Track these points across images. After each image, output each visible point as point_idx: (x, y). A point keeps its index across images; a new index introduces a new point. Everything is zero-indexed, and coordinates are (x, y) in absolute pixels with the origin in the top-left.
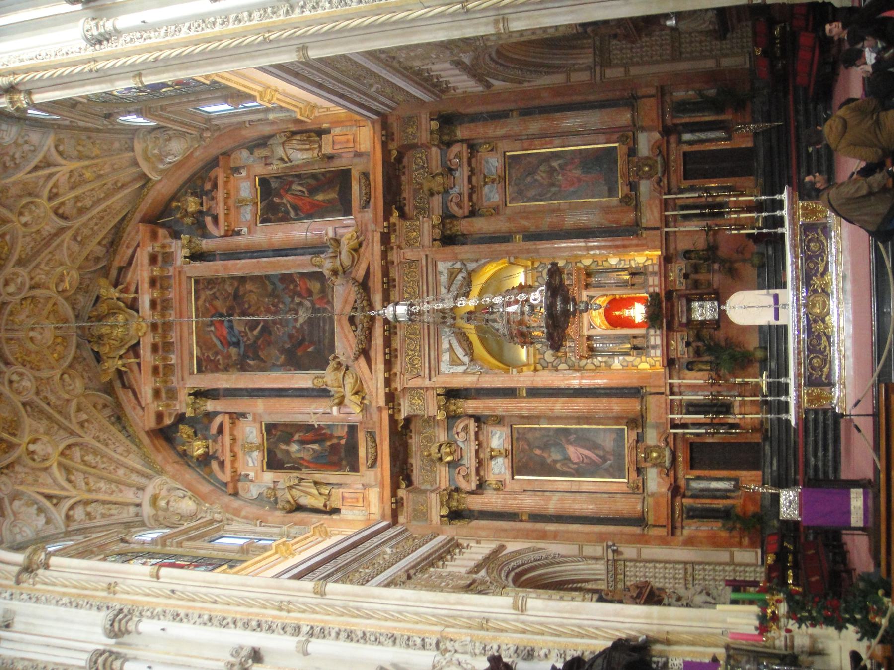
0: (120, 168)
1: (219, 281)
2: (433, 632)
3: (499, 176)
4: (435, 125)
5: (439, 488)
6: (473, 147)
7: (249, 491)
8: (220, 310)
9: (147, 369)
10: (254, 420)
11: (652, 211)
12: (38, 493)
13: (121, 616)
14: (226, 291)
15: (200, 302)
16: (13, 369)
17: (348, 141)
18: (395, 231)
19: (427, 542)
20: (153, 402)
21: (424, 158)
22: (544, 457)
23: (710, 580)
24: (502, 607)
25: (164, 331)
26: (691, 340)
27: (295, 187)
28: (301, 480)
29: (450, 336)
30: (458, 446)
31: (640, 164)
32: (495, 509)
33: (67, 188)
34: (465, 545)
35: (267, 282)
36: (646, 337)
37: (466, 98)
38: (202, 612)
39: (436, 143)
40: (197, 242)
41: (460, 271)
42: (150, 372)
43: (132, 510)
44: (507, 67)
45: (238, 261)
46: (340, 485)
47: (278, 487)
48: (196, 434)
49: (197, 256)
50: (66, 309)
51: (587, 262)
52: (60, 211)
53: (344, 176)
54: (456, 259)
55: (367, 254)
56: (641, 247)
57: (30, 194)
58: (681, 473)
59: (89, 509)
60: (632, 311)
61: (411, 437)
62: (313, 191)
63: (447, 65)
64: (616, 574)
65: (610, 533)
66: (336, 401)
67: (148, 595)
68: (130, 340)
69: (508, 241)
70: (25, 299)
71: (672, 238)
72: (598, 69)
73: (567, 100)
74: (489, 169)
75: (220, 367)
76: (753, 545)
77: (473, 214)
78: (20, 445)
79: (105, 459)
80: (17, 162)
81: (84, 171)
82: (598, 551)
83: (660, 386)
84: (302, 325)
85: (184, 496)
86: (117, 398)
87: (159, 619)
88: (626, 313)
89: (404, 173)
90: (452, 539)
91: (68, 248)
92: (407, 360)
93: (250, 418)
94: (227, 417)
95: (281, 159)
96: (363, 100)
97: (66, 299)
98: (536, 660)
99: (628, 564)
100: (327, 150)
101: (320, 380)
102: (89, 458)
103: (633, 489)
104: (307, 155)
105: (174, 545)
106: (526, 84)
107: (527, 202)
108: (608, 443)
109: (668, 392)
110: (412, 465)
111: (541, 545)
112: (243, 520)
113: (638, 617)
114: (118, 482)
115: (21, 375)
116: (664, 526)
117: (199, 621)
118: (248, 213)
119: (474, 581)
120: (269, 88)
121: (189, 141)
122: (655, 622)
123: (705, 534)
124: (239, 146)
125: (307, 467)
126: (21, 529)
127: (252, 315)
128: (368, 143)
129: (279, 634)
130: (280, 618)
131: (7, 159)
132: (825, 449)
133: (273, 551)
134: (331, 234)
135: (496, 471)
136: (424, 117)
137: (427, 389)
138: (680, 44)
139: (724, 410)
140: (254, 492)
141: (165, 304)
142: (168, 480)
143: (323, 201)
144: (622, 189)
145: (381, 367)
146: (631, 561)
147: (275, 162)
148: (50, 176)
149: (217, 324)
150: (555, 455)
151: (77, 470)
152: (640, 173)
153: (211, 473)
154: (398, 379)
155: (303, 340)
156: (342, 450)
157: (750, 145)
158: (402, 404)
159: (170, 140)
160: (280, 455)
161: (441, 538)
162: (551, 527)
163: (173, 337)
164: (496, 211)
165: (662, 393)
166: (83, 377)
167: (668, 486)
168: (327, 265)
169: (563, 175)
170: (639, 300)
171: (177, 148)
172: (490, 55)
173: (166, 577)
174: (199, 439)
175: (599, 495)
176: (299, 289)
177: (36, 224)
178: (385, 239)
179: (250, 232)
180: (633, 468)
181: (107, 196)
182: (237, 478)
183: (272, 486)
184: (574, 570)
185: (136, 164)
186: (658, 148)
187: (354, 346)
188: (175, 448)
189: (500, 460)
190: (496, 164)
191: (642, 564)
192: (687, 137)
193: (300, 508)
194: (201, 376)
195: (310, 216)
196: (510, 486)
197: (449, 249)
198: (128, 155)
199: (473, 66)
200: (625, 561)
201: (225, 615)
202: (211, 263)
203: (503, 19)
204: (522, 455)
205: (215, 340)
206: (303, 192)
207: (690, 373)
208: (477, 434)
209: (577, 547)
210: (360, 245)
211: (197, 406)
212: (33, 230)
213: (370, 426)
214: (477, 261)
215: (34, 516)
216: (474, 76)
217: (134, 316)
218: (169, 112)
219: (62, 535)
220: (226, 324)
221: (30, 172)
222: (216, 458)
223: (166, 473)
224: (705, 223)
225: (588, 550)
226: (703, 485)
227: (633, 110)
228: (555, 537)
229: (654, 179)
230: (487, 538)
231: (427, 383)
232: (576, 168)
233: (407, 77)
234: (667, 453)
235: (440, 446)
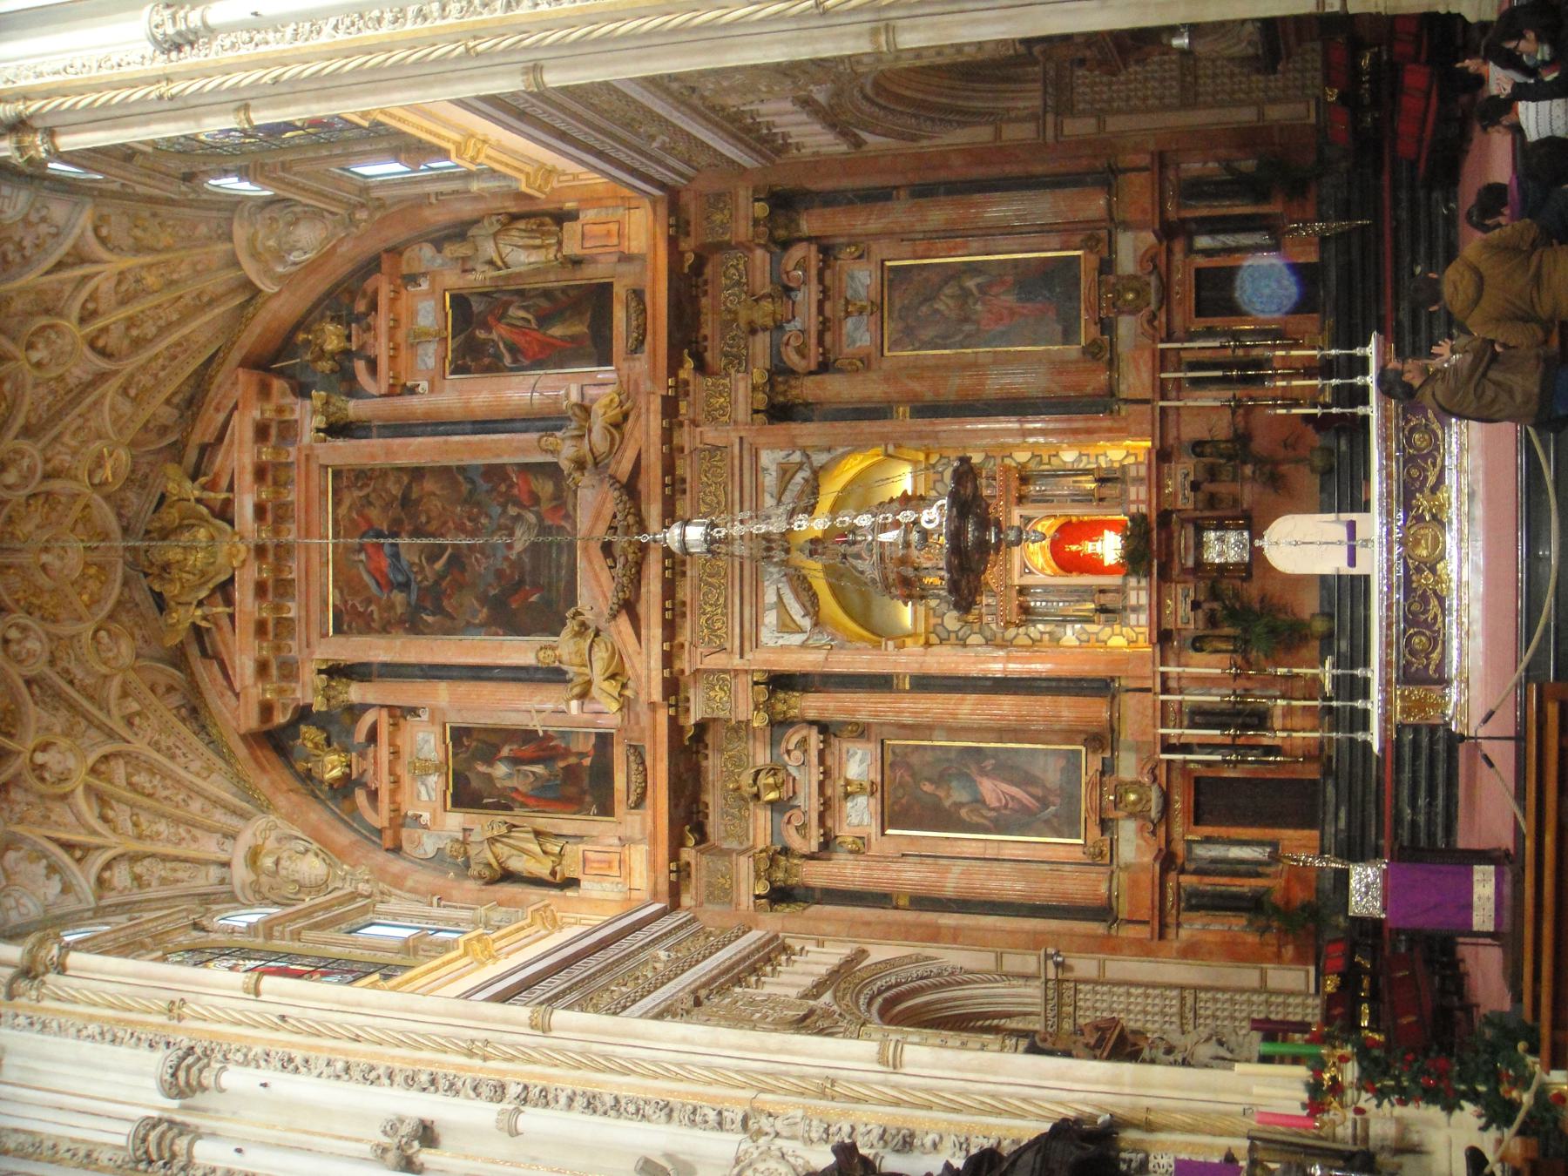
2: (738, 1101)
4: (761, 209)
5: (754, 847)
6: (827, 251)
9: (245, 625)
10: (432, 720)
11: (1138, 369)
12: (49, 838)
13: (190, 1060)
14: (388, 491)
15: (343, 510)
16: (11, 619)
17: (609, 234)
18: (687, 394)
19: (730, 942)
21: (741, 267)
22: (940, 799)
23: (1225, 1019)
24: (859, 1059)
25: (277, 557)
26: (1202, 598)
27: (515, 312)
30: (789, 774)
31: (1119, 287)
32: (851, 887)
33: (113, 302)
34: (798, 948)
35: (460, 478)
36: (1121, 590)
37: (818, 163)
38: (332, 1057)
40: (340, 404)
41: (800, 466)
42: (251, 628)
43: (214, 872)
44: (892, 111)
46: (579, 838)
47: (471, 839)
48: (329, 742)
49: (338, 429)
50: (105, 515)
51: (1022, 457)
52: (101, 343)
53: (603, 291)
54: (794, 447)
55: (636, 434)
56: (1119, 432)
57: (47, 312)
58: (1178, 830)
59: (138, 869)
60: (1098, 544)
61: (706, 757)
62: (544, 320)
63: (788, 105)
64: (1060, 1005)
65: (1052, 933)
66: (577, 690)
67: (238, 1023)
68: (218, 573)
69: (885, 418)
70: (35, 495)
71: (1172, 417)
72: (1050, 118)
73: (994, 171)
74: (855, 291)
76: (1300, 959)
77: (824, 367)
78: (19, 753)
79: (169, 782)
80: (27, 253)
81: (144, 274)
82: (1030, 963)
83: (1145, 678)
85: (307, 851)
86: (192, 674)
87: (258, 1067)
88: (1088, 547)
89: (705, 293)
90: (776, 937)
91: (113, 408)
92: (703, 620)
93: (425, 717)
94: (385, 713)
95: (491, 263)
96: (638, 162)
97: (107, 498)
98: (916, 1153)
99: (1081, 987)
100: (572, 248)
101: (549, 652)
102: (141, 779)
103: (1093, 856)
104: (535, 257)
105: (287, 936)
106: (925, 143)
108: (1052, 774)
109: (1158, 688)
110: (707, 806)
111: (930, 950)
112: (408, 895)
113: (1097, 1082)
114: (192, 824)
115: (24, 629)
117: (327, 1071)
118: (429, 357)
119: (811, 1012)
120: (472, 136)
122: (1127, 1090)
123: (1218, 938)
124: (421, 236)
125: (523, 805)
126: (17, 901)
127: (433, 535)
129: (468, 1097)
130: (470, 1069)
131: (10, 247)
132: (1432, 793)
133: (461, 951)
134: (574, 397)
136: (744, 194)
137: (736, 672)
138: (1196, 78)
139: (1255, 721)
140: (429, 846)
143: (562, 338)
144: (1087, 331)
145: (655, 631)
146: (1086, 982)
147: (480, 268)
148: (86, 279)
149: (370, 550)
150: (959, 794)
151: (119, 801)
152: (1119, 303)
153: (354, 811)
154: (686, 655)
155: (521, 582)
157: (1314, 259)
158: (692, 698)
160: (475, 783)
161: (754, 935)
162: (948, 920)
163: (294, 571)
164: (865, 363)
165: (1148, 690)
166: (132, 636)
168: (566, 451)
169: (984, 303)
170: (1112, 526)
171: (308, 238)
172: (862, 90)
173: (270, 993)
175: (1034, 866)
176: (516, 491)
177: (57, 365)
178: (670, 408)
179: (432, 390)
180: (1094, 818)
182: (399, 820)
183: (460, 836)
184: (986, 996)
185: (235, 263)
186: (1152, 259)
187: (609, 595)
188: (290, 765)
189: (862, 800)
190: (868, 281)
192: (1203, 242)
193: (508, 876)
194: (341, 639)
195: (539, 364)
196: (877, 846)
197: (781, 429)
198: (221, 247)
199: (831, 107)
200: (1076, 981)
201: (374, 1062)
202: (364, 441)
203: (887, 26)
204: (900, 792)
205: (366, 577)
206: (528, 321)
207: (1198, 656)
208: (821, 753)
209: (993, 955)
210: (626, 416)
211: (332, 693)
212: (53, 375)
213: (636, 735)
214: (829, 450)
215: (42, 879)
216: (833, 126)
217: (225, 532)
219: (90, 914)
220: (387, 549)
221: (48, 273)
222: (365, 785)
223: (276, 809)
224: (1230, 394)
225: (1013, 962)
226: (1216, 851)
227: (1109, 193)
228: (955, 937)
229: (1145, 312)
230: (837, 938)
231: (737, 662)
233: (716, 125)
234: (1154, 795)
235: (757, 773)
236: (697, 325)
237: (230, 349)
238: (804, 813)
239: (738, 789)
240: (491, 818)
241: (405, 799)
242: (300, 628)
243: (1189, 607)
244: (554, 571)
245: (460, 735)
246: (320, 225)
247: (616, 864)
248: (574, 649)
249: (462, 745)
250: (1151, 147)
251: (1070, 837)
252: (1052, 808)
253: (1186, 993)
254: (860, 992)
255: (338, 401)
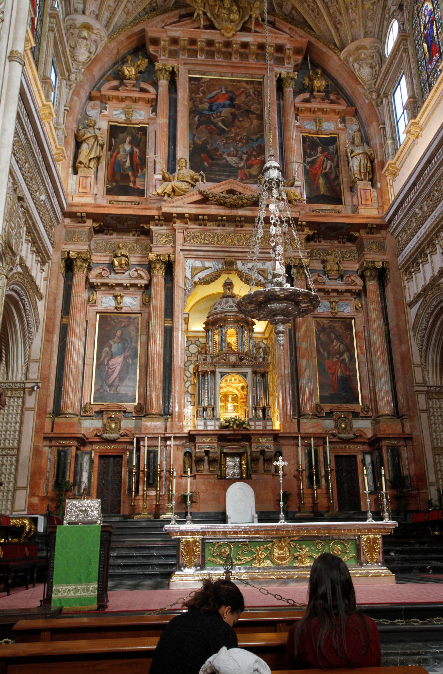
0: (352, 27)
1: (260, 100)
3: (336, 313)
4: (379, 265)
7: (93, 109)
8: (238, 99)
10: (150, 119)
14: (252, 104)
17: (367, 200)
20: (168, 36)
21: (351, 258)
22: (114, 338)
25: (224, 53)
28: (102, 146)
29: (215, 268)
30: (126, 271)
31: (347, 421)
34: (44, 268)
35: (258, 136)
37: (401, 288)
39: (365, 265)
41: (266, 278)
42: (193, 36)
44: (429, 317)
45: (276, 112)
46: (96, 178)
53: (338, 200)
56: (284, 418)
58: (96, 447)
61: (134, 235)
66: (167, 176)
71: (292, 442)
72: (425, 389)
73: (397, 365)
75: (193, 95)
82: (34, 375)
84: (225, 159)
85: (90, 53)
86: (172, 10)
89: (339, 242)
90: (49, 259)
92: (197, 233)
93: (152, 115)
94: (154, 96)
95: (352, 152)
96: (407, 205)
99: (21, 400)
100: (360, 185)
101: (184, 164)
103: (85, 407)
104: (356, 169)
105: (51, 25)
106: (412, 334)
107: (316, 333)
110: (111, 235)
112: (69, 97)
116: (52, 431)
121: (370, 82)
123: (43, 465)
125: (111, 156)
128: (366, 214)
133: (45, 103)
135: (104, 300)
136: (385, 257)
137: (174, 248)
139: (151, 482)
140: (93, 113)
141: (244, 56)
142: (104, 42)
143: (318, 183)
144: (327, 408)
146: (23, 402)
150: (115, 347)
153: (108, 80)
155: (213, 159)
156: (124, 184)
158: (162, 228)
159: (371, 67)
160: (121, 136)
163: (218, 59)
165: (166, 430)
167: (87, 436)
169: (336, 362)
174: (136, 74)
175: (80, 380)
176: (253, 159)
180: (103, 408)
181: (330, 15)
183: (97, 126)
185: (353, 40)
189: (113, 303)
191: (19, 411)
192: (368, 459)
193: (78, 145)
194: (187, 79)
196: (92, 310)
200: (24, 398)
205: (214, 93)
209: (38, 358)
211: (164, 72)
216: (425, 290)
218: (402, 56)
223: (110, 42)
225: (34, 368)
226: (86, 466)
227: (391, 415)
228: (48, 341)
230: (48, 286)
231: (179, 247)
232: (342, 372)
234: (115, 436)
235: (127, 257)
236: (327, 238)
237: (316, 38)
238: (108, 277)
239: (119, 248)
240: (106, 138)
241: (114, 103)
242: (192, 60)
243: (206, 449)
244: (218, 173)
245: (144, 130)
246: (370, 78)
247: (85, 191)
248: (185, 175)
249: (139, 131)
250: (414, 434)
251: (94, 397)
252: (108, 389)
253: (15, 451)
254: (22, 289)
255: (292, 83)
